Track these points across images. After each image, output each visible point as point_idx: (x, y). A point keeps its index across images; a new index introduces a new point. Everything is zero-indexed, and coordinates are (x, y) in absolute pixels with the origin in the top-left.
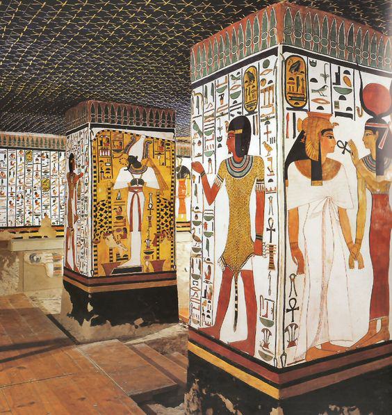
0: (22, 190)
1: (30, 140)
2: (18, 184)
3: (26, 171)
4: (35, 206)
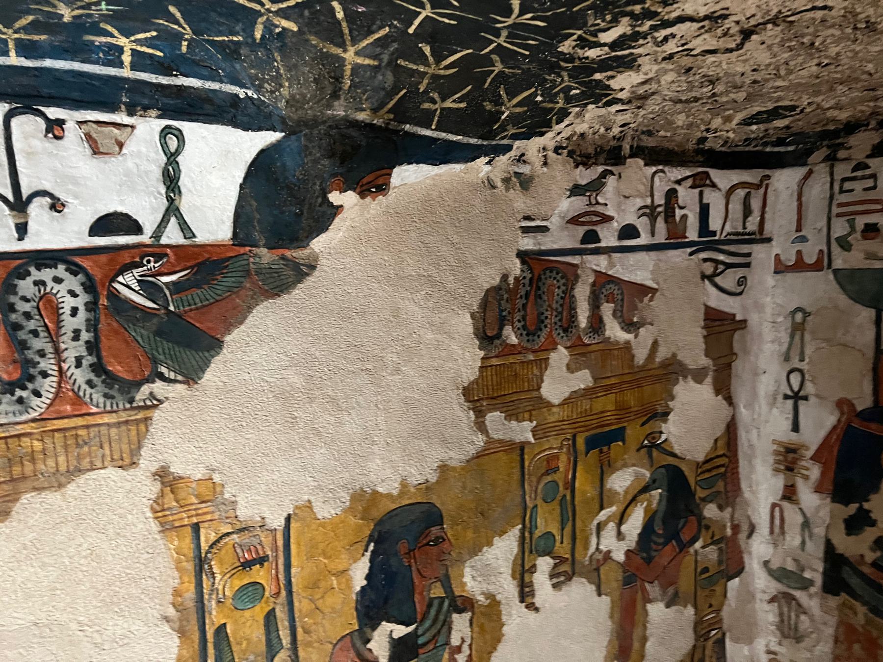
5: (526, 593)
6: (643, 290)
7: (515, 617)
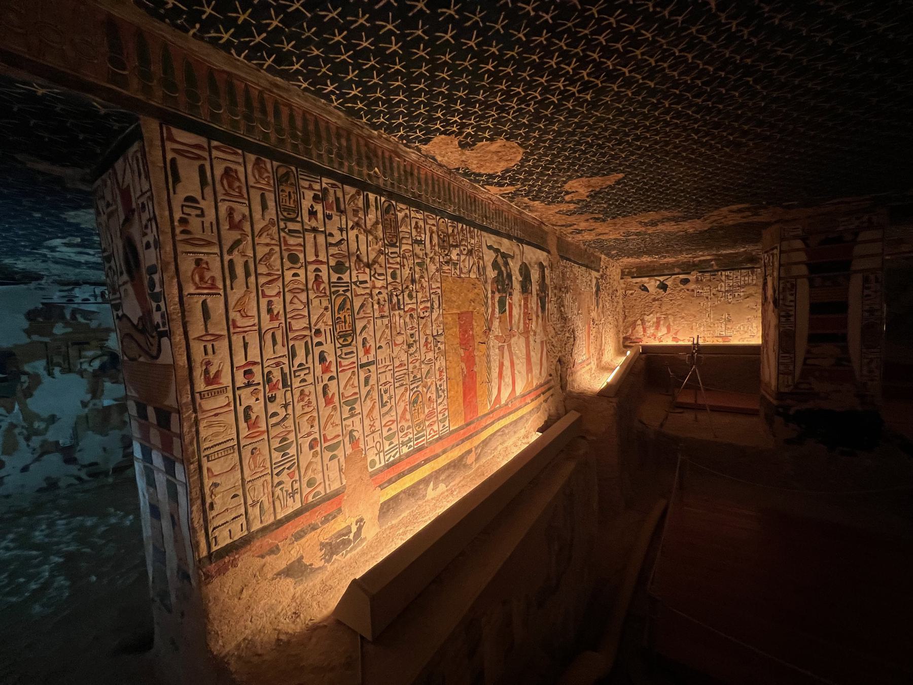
0: (282, 351)
1: (285, 111)
2: (266, 323)
3: (287, 264)
4: (325, 412)
5: (50, 374)
6: (93, 312)
7: (46, 380)
